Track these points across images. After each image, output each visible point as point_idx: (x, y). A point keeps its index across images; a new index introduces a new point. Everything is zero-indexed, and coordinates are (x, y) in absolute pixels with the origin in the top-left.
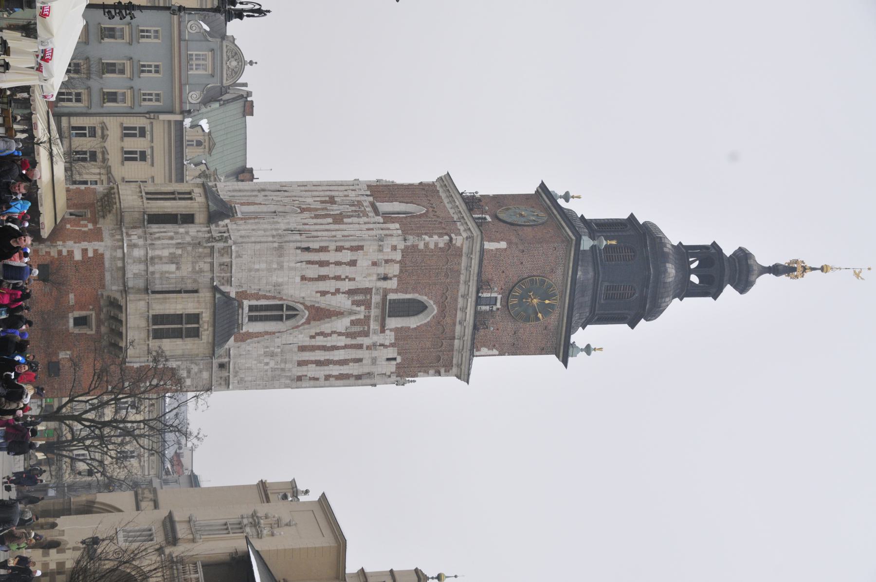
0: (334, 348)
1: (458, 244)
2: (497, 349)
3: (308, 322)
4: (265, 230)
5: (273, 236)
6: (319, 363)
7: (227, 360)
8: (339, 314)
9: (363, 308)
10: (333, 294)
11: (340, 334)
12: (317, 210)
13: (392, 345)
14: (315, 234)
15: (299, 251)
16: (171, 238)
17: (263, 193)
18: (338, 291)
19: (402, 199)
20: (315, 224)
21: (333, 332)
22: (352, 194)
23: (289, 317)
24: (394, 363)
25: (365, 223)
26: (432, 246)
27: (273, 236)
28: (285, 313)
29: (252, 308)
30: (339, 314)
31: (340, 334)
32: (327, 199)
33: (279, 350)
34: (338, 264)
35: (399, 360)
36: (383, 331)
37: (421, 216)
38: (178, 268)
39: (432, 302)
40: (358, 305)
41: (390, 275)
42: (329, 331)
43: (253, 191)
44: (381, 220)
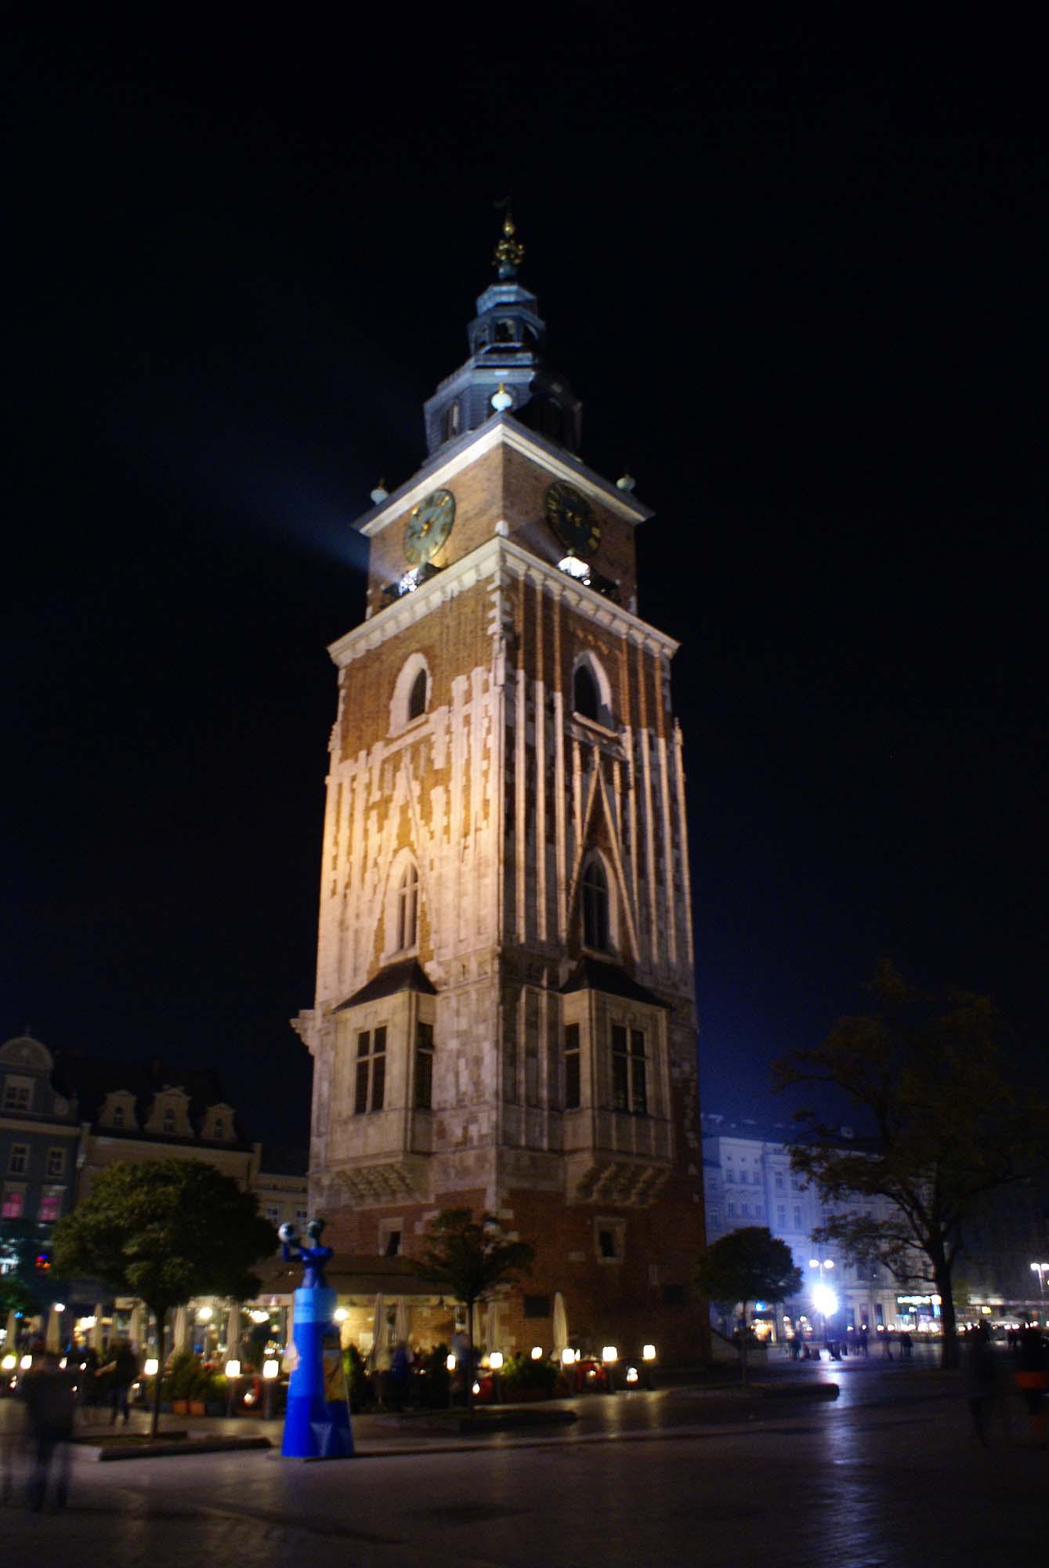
1: (508, 581)
3: (609, 851)
4: (460, 895)
5: (480, 876)
6: (659, 852)
12: (405, 823)
16: (478, 1061)
17: (352, 922)
18: (569, 788)
19: (383, 700)
20: (447, 813)
22: (363, 778)
23: (602, 882)
25: (448, 731)
27: (480, 876)
29: (589, 942)
32: (374, 814)
43: (342, 940)
44: (444, 709)
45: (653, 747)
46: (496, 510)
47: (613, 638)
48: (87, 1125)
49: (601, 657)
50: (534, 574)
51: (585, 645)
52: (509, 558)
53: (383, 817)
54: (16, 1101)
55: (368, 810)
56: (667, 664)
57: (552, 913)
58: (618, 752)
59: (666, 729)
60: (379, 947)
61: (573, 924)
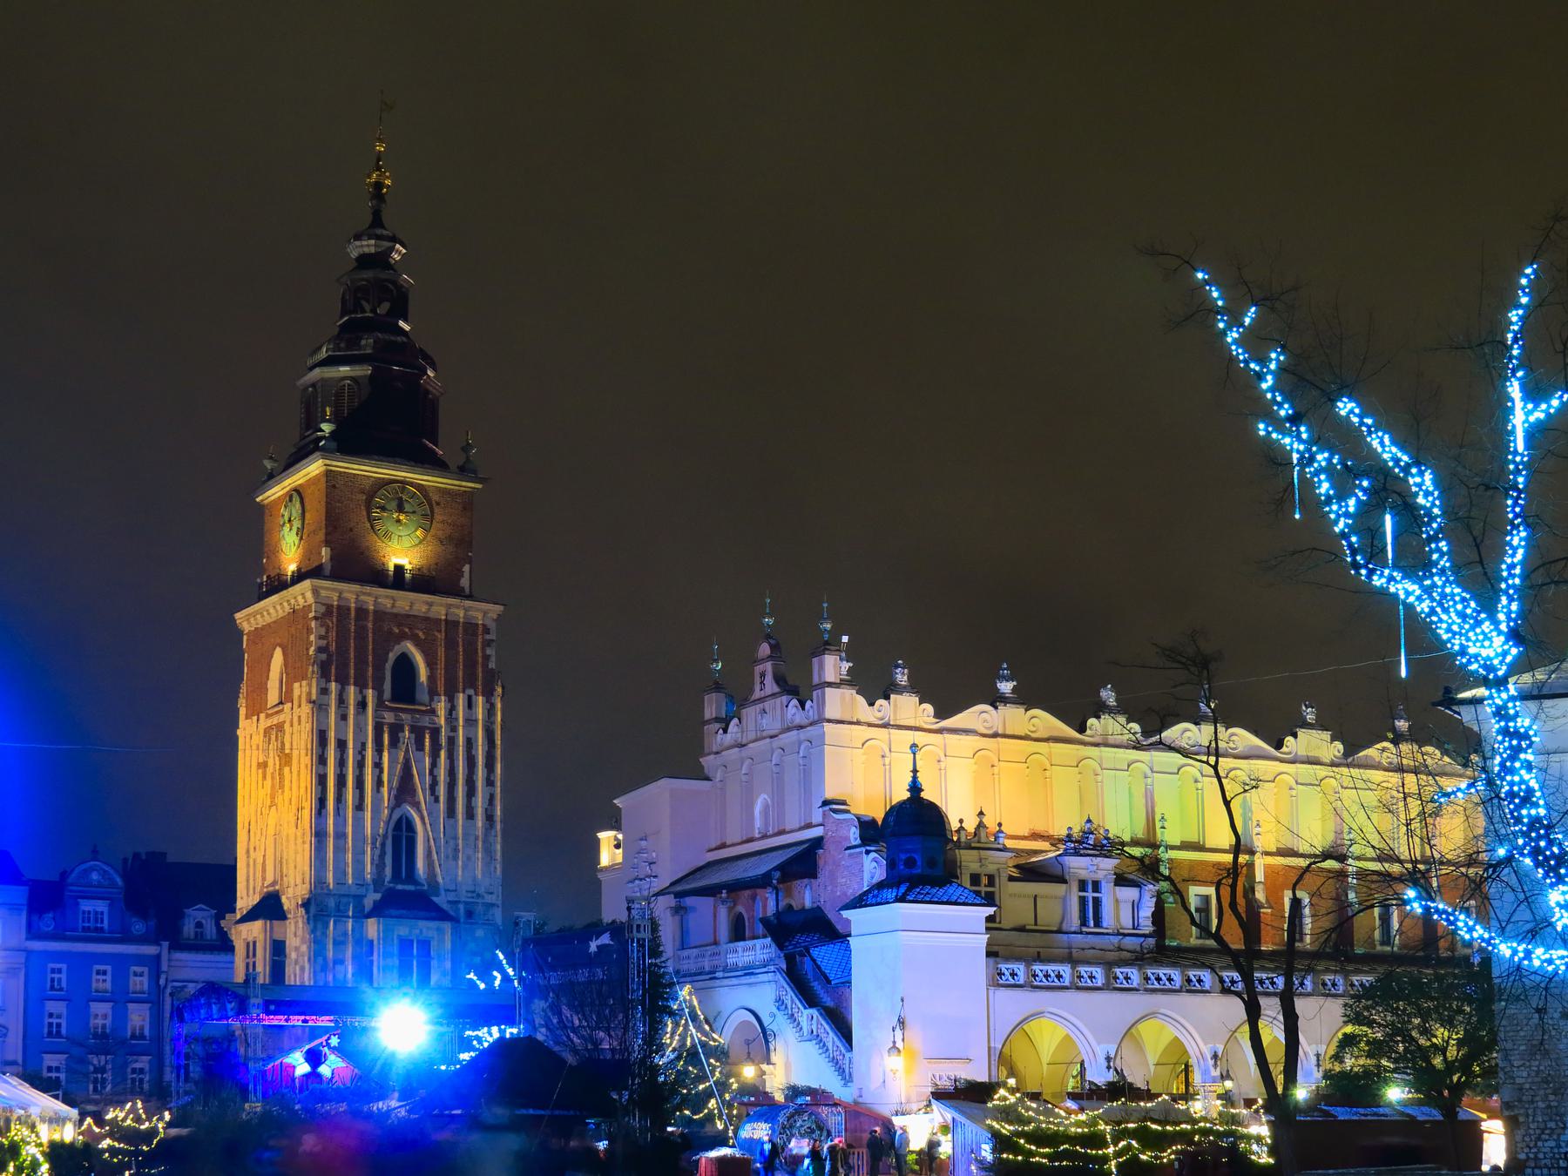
0: (452, 772)
1: (323, 609)
3: (417, 805)
7: (461, 907)
10: (381, 771)
11: (434, 764)
12: (273, 786)
14: (302, 790)
16: (302, 969)
18: (378, 765)
23: (411, 828)
31: (434, 764)
34: (342, 763)
35: (471, 692)
36: (433, 712)
37: (285, 654)
45: (470, 704)
46: (321, 536)
47: (429, 622)
48: (166, 944)
49: (419, 644)
50: (345, 595)
51: (402, 637)
52: (323, 593)
53: (264, 777)
54: (92, 925)
55: (259, 765)
56: (492, 626)
57: (359, 862)
59: (484, 686)
60: (264, 879)
61: (379, 866)
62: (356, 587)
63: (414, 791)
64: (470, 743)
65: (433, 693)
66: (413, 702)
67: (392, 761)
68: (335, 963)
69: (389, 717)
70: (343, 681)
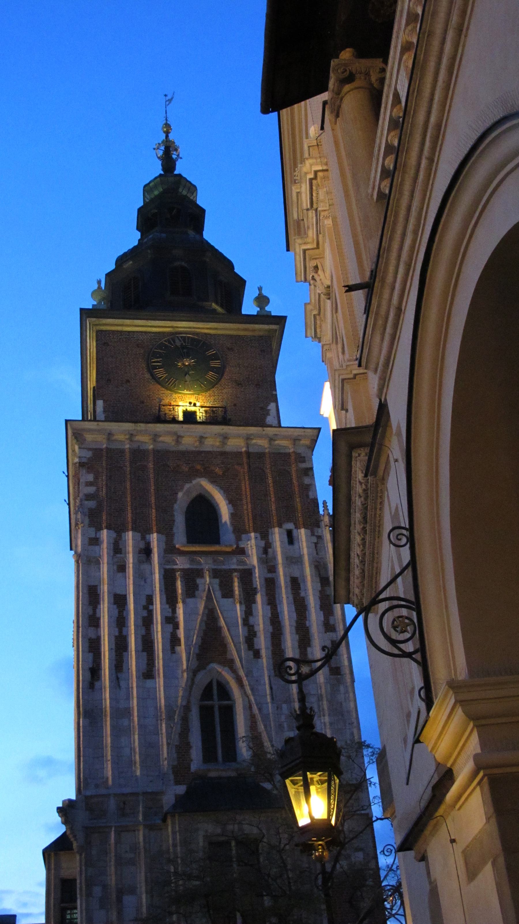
0: (275, 621)
1: (89, 454)
2: (268, 404)
3: (230, 664)
8: (211, 617)
9: (199, 581)
10: (176, 626)
11: (249, 612)
13: (265, 536)
15: (97, 684)
18: (170, 620)
21: (246, 622)
24: (295, 532)
26: (91, 490)
28: (216, 703)
30: (211, 617)
31: (249, 612)
33: (285, 706)
34: (120, 622)
35: (290, 526)
38: (133, 891)
39: (187, 486)
40: (195, 587)
41: (142, 545)
42: (246, 628)
49: (214, 480)
58: (244, 563)
61: (182, 749)
62: (128, 426)
63: (224, 646)
64: (295, 584)
65: (240, 531)
66: (216, 540)
67: (189, 615)
68: (120, 893)
69: (181, 563)
70: (119, 530)
